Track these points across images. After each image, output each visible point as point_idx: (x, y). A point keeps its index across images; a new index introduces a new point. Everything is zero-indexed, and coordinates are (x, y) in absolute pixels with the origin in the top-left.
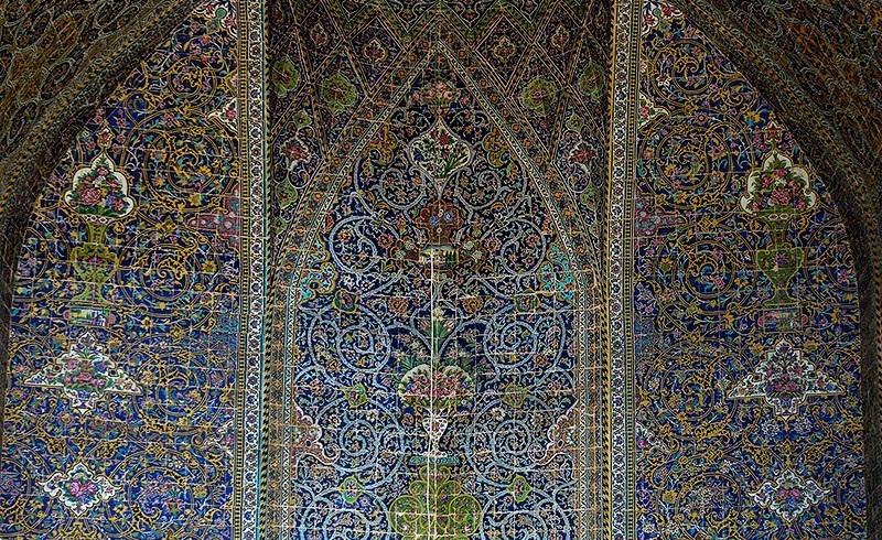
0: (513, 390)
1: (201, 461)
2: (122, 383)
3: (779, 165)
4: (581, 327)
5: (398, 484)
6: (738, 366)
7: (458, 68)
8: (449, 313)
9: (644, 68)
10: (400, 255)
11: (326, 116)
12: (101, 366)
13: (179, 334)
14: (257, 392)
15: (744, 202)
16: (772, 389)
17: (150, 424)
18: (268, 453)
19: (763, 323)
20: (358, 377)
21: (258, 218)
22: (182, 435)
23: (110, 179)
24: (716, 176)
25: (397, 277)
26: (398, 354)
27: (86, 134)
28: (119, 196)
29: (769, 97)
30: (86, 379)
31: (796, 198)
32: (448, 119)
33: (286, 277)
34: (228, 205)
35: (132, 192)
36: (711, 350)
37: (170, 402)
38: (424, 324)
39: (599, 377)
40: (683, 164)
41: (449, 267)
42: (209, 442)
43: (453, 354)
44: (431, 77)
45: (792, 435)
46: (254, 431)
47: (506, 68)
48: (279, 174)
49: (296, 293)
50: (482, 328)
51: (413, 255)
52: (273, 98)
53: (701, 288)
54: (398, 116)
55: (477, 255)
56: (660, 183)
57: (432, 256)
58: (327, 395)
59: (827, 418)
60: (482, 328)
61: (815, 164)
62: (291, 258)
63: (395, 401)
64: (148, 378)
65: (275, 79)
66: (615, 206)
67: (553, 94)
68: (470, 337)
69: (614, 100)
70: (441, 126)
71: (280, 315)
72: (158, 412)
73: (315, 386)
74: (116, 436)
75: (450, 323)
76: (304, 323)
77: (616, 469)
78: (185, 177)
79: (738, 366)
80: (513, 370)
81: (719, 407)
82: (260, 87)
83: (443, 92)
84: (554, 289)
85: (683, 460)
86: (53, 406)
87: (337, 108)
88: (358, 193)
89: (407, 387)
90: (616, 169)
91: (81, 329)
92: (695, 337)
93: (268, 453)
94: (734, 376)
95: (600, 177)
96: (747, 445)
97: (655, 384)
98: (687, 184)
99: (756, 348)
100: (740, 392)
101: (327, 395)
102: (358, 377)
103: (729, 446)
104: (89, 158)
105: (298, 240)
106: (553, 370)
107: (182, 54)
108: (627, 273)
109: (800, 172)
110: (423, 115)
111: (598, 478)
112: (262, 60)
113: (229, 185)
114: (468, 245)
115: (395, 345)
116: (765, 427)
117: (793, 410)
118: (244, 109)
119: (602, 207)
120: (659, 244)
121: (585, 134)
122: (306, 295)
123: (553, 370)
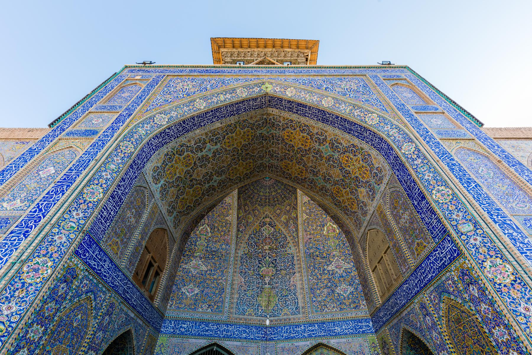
0: (283, 272)
1: (218, 285)
2: (204, 268)
3: (330, 225)
4: (295, 258)
5: (260, 292)
6: (328, 263)
7: (270, 216)
8: (270, 258)
9: (304, 208)
10: (260, 247)
11: (247, 222)
12: (200, 264)
13: (216, 259)
14: (231, 271)
15: (325, 232)
16: (336, 267)
17: (208, 277)
18: (232, 284)
19: (332, 254)
20: (252, 269)
21: (234, 238)
22: (215, 279)
23: (207, 229)
24: (319, 228)
25: (260, 251)
26: (260, 265)
27: (203, 220)
28: (208, 233)
29: (326, 211)
30: (196, 267)
31: (334, 231)
32: (269, 224)
33: (239, 249)
34: (228, 235)
35: (211, 232)
36: (322, 260)
37: (213, 272)
38: (265, 260)
39: (300, 268)
40: (312, 226)
41: (270, 249)
42: (220, 281)
43: (270, 265)
44: (266, 217)
45: (342, 277)
46: (230, 279)
47: (278, 215)
48: (238, 230)
49: (240, 253)
50: (276, 260)
51: (263, 247)
52: (238, 215)
53: (318, 249)
54: (260, 223)
55: (275, 247)
56: (308, 230)
57: (266, 247)
58: (245, 273)
59: (349, 272)
60: (276, 260)
61: (337, 224)
62: (240, 246)
63: (259, 274)
64: (209, 267)
65: (238, 213)
66: (300, 234)
67: (287, 218)
68: (274, 262)
69: (299, 215)
70: (267, 225)
71: (237, 257)
72: (210, 274)
73: (243, 271)
74: (201, 280)
75: (270, 259)
76: (242, 258)
77: (306, 286)
78: (221, 229)
79: (328, 263)
80: (283, 268)
81: (326, 272)
82: (235, 213)
83: (268, 220)
84: (290, 251)
85: (320, 283)
86: (188, 272)
87: (249, 221)
88: (253, 236)
89: (262, 272)
90: (300, 227)
91: (197, 257)
92: (318, 258)
93: (232, 284)
94: (328, 265)
95: (297, 230)
96: (333, 279)
97: (312, 268)
98: (313, 230)
99: (331, 260)
100: (330, 268)
101: (245, 273)
102: (252, 269)
103: (329, 280)
104: (203, 225)
105: (241, 243)
106: (291, 267)
107: (222, 207)
108: (304, 247)
109: (334, 226)
110: (265, 224)
111: (302, 289)
112: (236, 208)
113: (229, 231)
114: (273, 245)
115: (259, 263)
116: (336, 275)
117: (342, 271)
118: (232, 217)
119: (298, 235)
120: (309, 241)
121: (294, 223)
122: (243, 253)
123: (291, 267)
